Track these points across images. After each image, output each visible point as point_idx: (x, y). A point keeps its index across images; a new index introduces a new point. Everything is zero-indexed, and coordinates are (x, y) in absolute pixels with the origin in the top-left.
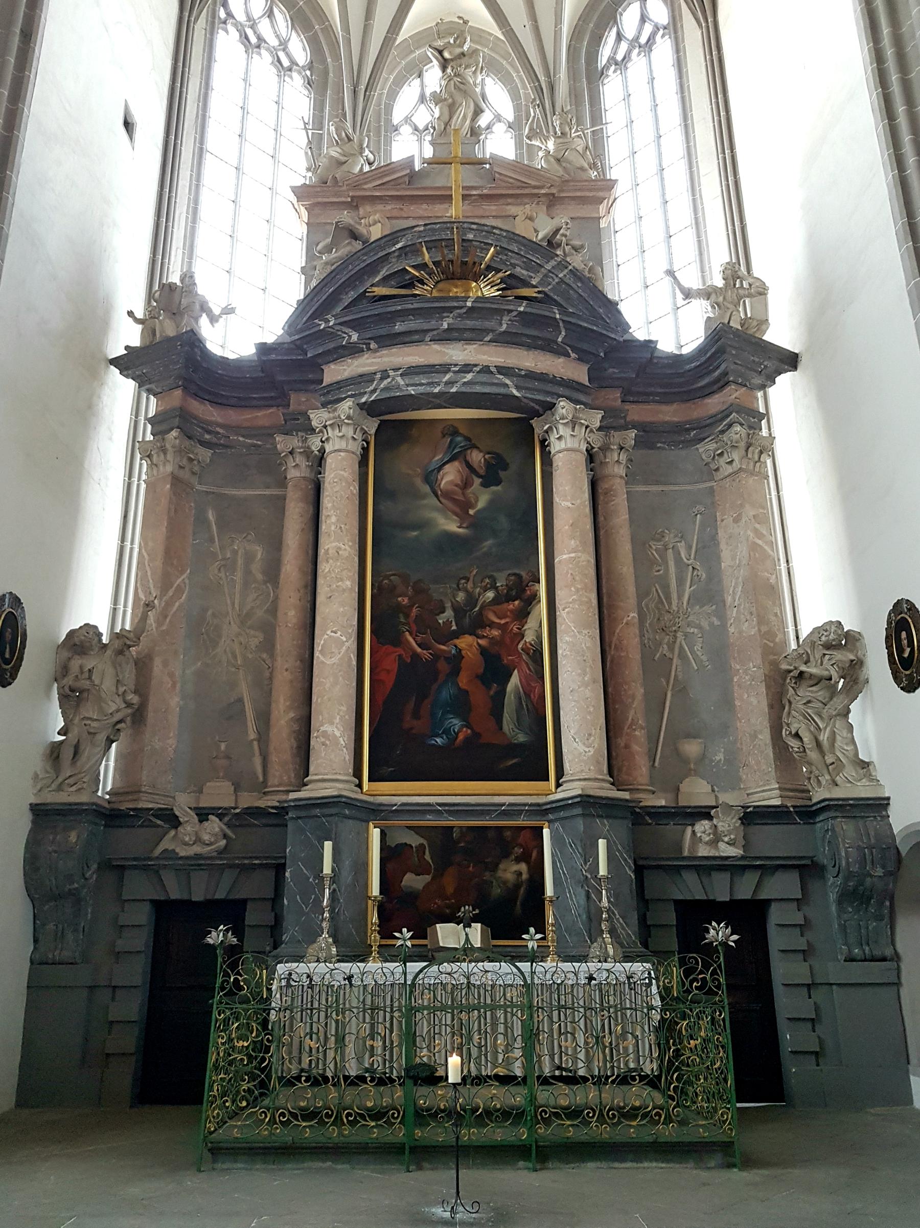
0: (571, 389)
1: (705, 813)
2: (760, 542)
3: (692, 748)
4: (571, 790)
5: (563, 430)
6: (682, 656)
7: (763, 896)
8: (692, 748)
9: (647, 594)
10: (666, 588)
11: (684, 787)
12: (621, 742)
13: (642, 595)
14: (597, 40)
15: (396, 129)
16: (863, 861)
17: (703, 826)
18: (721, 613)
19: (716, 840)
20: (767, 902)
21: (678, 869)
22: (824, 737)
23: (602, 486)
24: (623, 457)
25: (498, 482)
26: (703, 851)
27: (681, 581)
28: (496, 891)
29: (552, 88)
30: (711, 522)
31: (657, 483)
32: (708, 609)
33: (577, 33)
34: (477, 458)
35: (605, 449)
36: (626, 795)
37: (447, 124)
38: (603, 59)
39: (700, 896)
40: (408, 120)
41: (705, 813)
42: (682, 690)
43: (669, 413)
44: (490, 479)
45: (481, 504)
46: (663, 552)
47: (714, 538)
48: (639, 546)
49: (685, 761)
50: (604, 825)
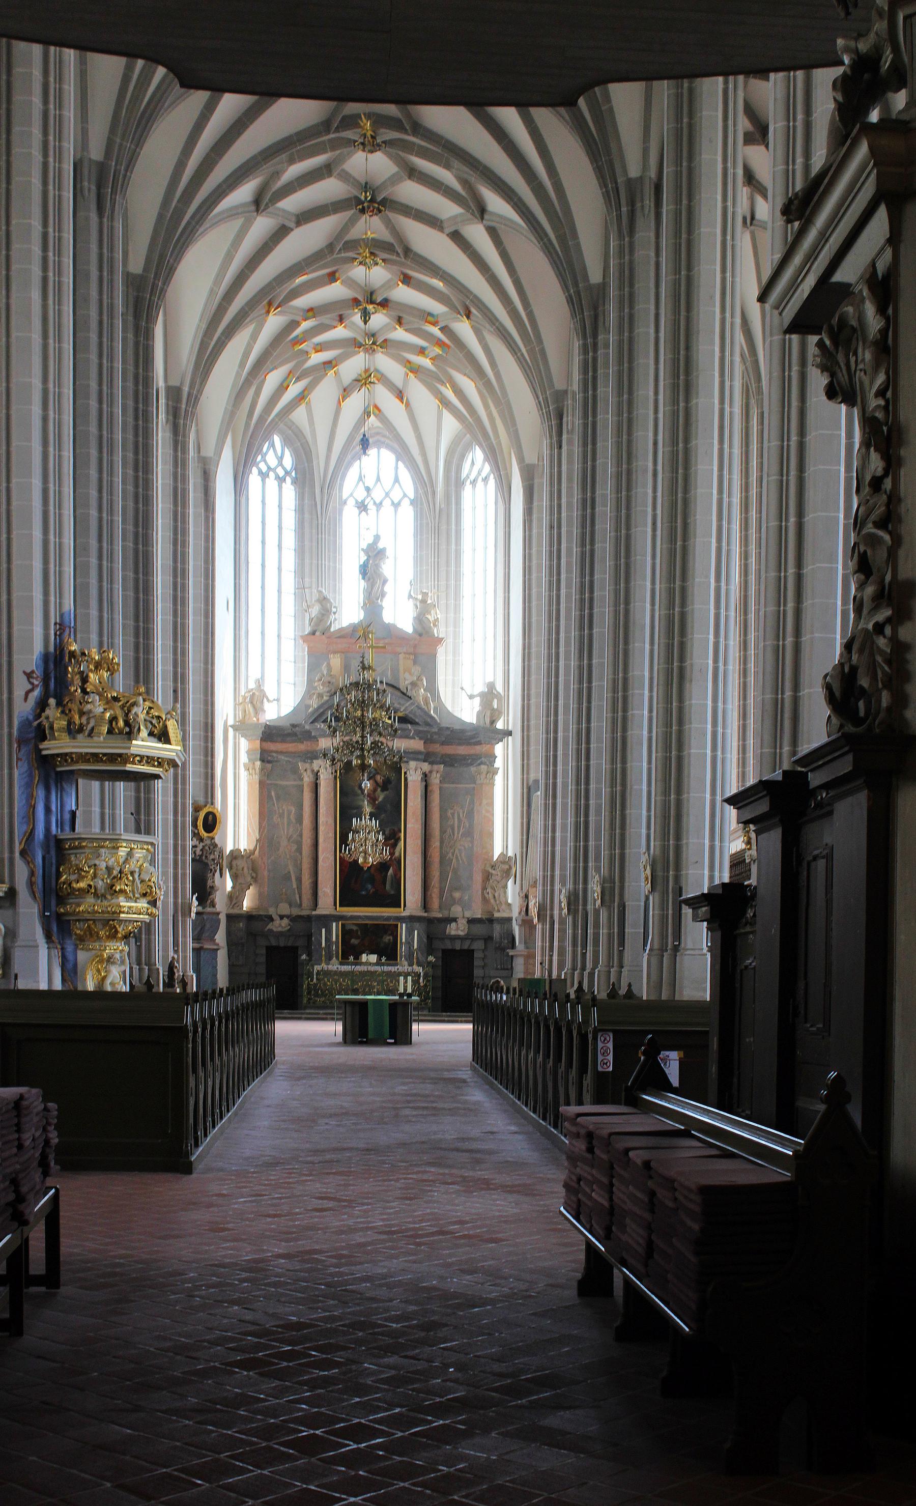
0: (415, 755)
1: (455, 920)
2: (488, 815)
3: (457, 895)
4: (406, 913)
5: (412, 772)
6: (457, 858)
7: (472, 948)
8: (457, 895)
9: (445, 832)
10: (453, 829)
11: (452, 909)
12: (429, 893)
13: (443, 831)
14: (462, 457)
15: (345, 503)
16: (501, 938)
17: (453, 925)
18: (472, 842)
19: (457, 929)
20: (473, 951)
21: (443, 939)
22: (496, 895)
23: (429, 788)
24: (438, 775)
25: (387, 790)
26: (453, 933)
27: (459, 827)
28: (382, 945)
29: (434, 493)
30: (472, 802)
31: (453, 783)
32: (469, 839)
33: (451, 452)
34: (379, 778)
35: (431, 772)
36: (426, 915)
37: (370, 594)
38: (464, 475)
39: (450, 947)
40: (351, 495)
41: (455, 920)
42: (455, 871)
43: (462, 750)
44: (384, 787)
45: (380, 799)
46: (453, 814)
47: (473, 809)
48: (443, 810)
49: (454, 899)
50: (417, 925)
